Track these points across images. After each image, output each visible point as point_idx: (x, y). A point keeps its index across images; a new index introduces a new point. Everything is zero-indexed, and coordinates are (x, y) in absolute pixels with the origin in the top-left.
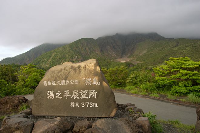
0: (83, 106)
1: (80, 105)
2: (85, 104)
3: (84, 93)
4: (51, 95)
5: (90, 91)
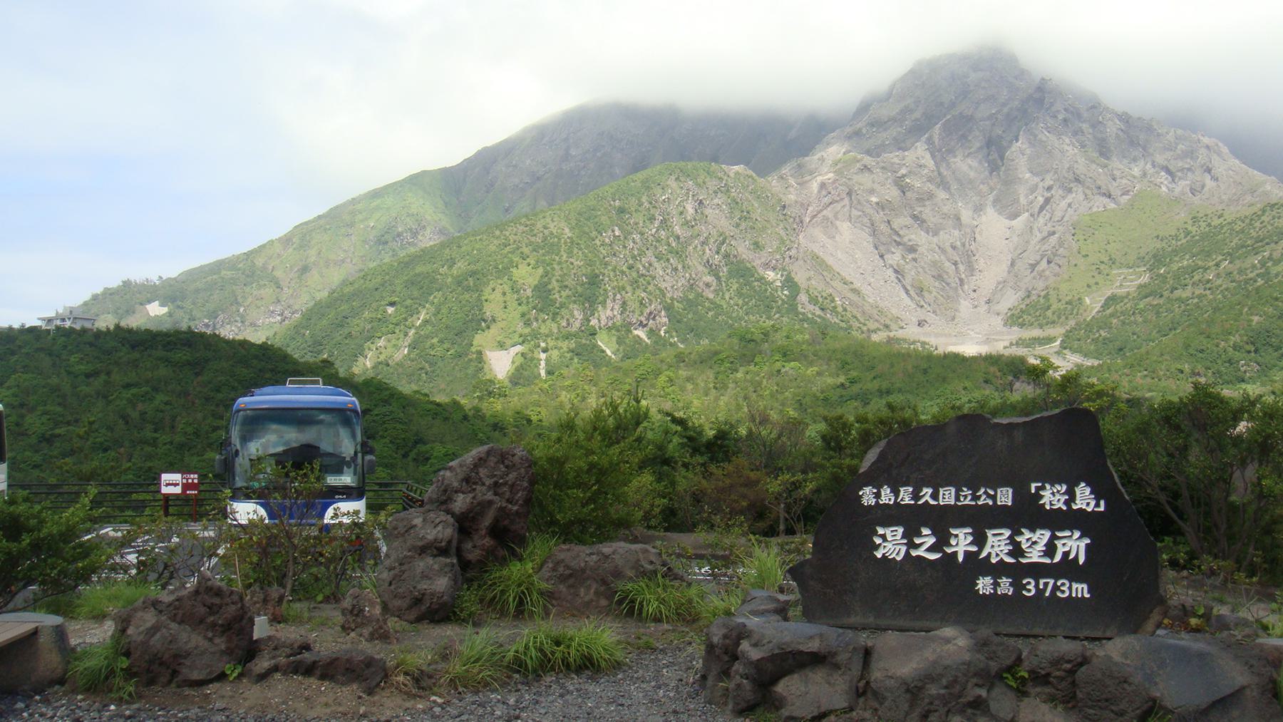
0: (1029, 591)
1: (1018, 586)
2: (1037, 586)
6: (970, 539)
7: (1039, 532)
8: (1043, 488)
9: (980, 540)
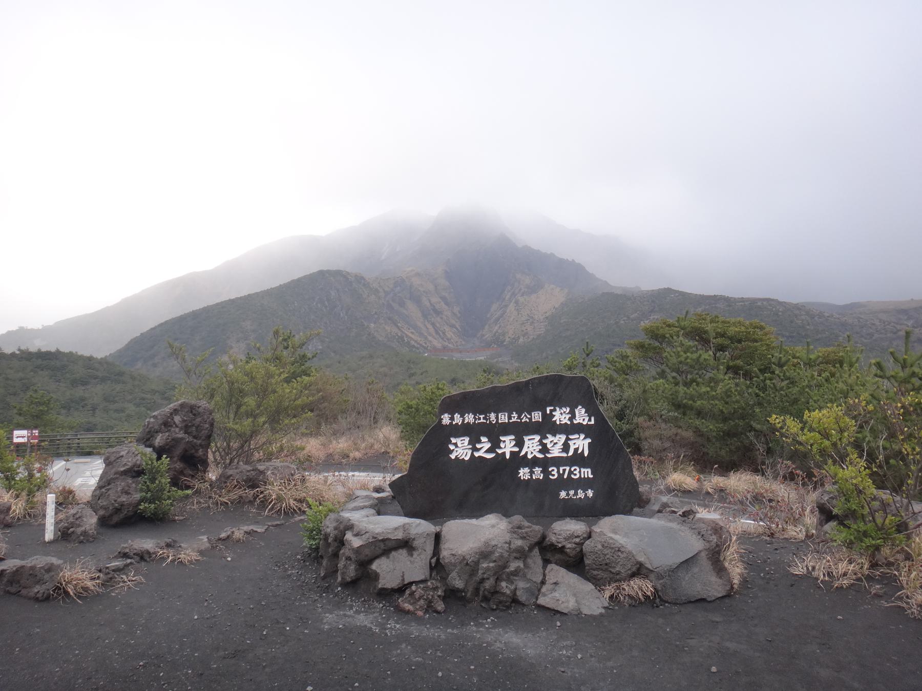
0: (553, 475)
2: (558, 471)
3: (556, 443)
4: (460, 451)
5: (571, 437)
6: (513, 443)
7: (558, 436)
8: (555, 410)
9: (520, 444)
